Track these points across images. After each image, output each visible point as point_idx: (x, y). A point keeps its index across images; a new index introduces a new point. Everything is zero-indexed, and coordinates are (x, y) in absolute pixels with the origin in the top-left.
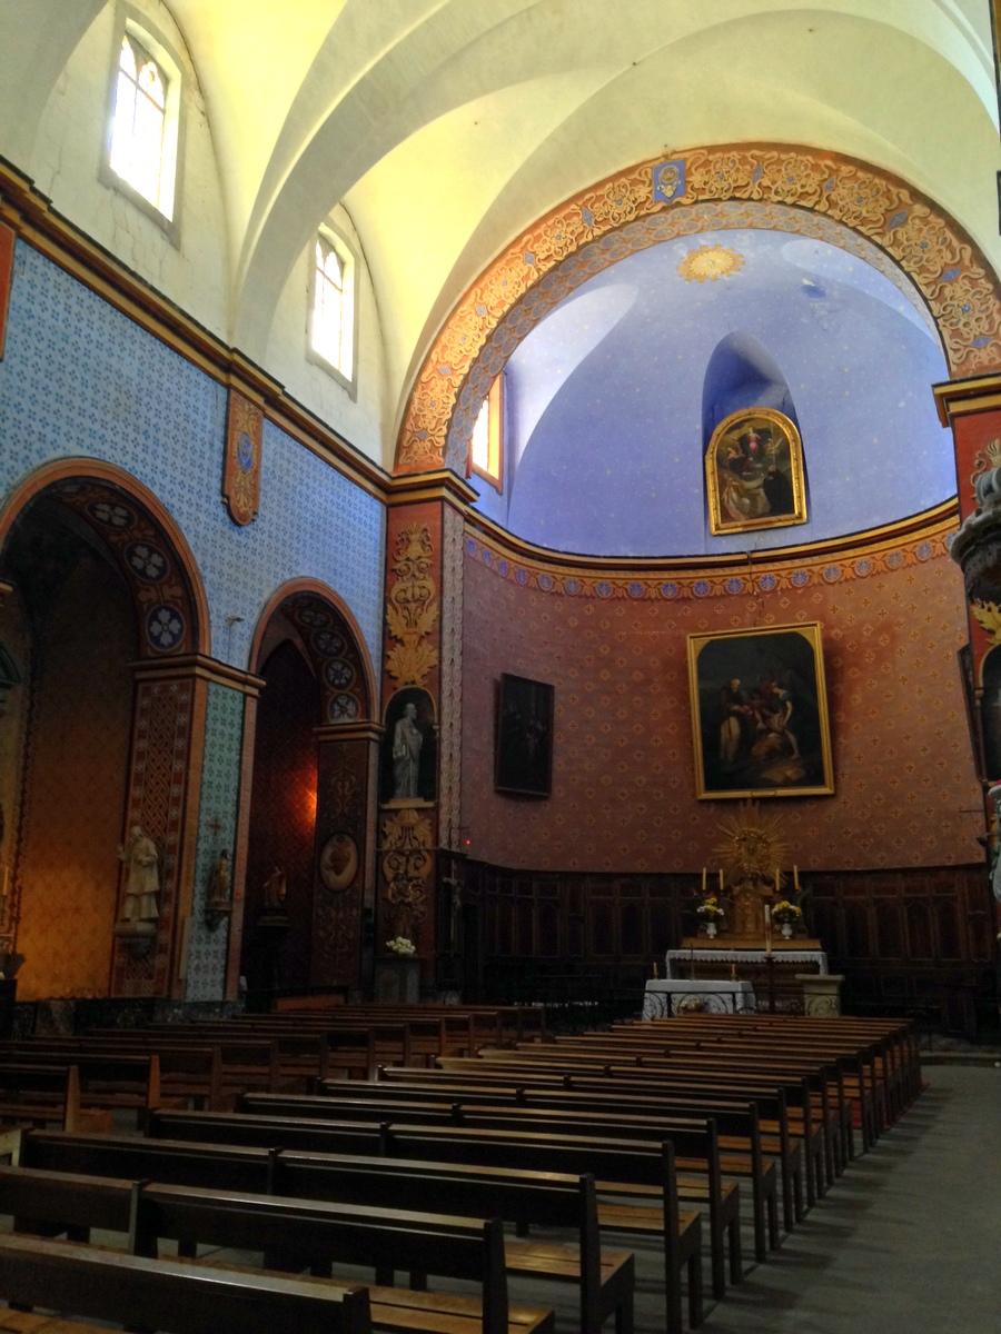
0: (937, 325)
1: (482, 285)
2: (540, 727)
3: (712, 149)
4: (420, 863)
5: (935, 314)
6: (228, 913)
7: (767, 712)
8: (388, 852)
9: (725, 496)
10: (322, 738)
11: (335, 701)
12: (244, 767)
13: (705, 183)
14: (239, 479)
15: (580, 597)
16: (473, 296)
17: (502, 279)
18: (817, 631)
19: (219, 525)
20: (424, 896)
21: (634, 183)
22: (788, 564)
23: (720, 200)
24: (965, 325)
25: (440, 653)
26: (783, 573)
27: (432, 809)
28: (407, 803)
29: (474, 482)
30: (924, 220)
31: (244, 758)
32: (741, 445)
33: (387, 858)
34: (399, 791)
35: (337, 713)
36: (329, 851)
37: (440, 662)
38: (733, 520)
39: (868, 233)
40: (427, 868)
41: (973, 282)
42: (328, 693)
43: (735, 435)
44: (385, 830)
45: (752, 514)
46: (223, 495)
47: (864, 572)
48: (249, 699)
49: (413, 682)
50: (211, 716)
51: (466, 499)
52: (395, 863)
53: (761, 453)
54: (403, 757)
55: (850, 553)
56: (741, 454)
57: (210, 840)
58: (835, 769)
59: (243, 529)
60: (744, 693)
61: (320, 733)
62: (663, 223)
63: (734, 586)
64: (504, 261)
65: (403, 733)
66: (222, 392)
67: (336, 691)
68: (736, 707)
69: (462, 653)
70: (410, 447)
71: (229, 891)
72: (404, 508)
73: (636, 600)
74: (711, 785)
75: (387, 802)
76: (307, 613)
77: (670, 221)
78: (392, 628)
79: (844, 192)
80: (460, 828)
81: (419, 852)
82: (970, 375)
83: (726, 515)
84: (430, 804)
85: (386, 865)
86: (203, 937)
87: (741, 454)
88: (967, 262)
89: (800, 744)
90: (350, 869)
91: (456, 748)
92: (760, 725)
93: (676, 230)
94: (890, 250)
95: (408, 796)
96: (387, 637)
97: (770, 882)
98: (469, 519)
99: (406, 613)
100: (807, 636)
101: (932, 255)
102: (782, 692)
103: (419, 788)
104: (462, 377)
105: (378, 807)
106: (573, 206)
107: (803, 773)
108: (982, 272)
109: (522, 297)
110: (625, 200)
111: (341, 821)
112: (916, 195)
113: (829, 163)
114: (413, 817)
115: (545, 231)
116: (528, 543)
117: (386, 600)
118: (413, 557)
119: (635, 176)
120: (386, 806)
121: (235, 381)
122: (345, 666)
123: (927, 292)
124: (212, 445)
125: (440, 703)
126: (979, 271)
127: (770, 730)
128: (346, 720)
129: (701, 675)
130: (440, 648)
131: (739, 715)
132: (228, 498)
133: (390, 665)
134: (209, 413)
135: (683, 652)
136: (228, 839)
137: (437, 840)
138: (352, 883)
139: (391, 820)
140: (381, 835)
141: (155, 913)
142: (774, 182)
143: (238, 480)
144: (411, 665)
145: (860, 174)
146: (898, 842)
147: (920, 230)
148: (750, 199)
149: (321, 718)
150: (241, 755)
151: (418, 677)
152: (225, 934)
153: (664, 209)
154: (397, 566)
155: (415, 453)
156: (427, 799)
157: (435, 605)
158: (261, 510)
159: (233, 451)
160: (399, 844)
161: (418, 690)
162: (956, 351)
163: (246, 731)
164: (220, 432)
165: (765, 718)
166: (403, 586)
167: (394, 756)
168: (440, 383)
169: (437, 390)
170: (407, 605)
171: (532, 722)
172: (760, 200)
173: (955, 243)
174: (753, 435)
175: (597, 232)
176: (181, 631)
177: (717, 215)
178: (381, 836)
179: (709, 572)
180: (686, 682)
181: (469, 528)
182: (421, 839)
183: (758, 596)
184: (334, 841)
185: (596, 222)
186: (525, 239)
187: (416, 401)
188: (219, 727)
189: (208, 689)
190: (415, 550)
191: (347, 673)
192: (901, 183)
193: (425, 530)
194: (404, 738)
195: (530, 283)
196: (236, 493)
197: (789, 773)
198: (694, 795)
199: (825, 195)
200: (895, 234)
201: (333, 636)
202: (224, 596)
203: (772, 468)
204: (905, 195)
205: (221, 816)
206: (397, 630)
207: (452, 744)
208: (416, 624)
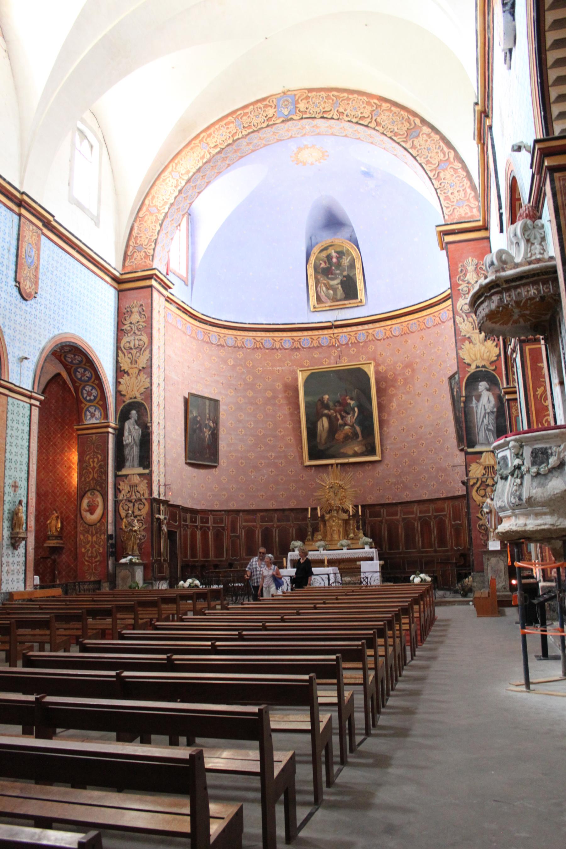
0: (437, 193)
1: (176, 161)
2: (212, 424)
3: (310, 90)
5: (436, 187)
6: (24, 539)
8: (122, 501)
9: (319, 289)
10: (80, 432)
11: (87, 410)
12: (31, 450)
13: (307, 108)
14: (25, 272)
15: (235, 347)
16: (170, 169)
18: (372, 366)
19: (13, 300)
20: (144, 526)
21: (266, 106)
22: (355, 328)
23: (315, 118)
24: (452, 194)
25: (151, 379)
26: (352, 334)
27: (148, 474)
28: (132, 470)
29: (171, 277)
30: (428, 135)
31: (31, 445)
32: (328, 260)
33: (121, 504)
34: (128, 464)
35: (89, 417)
36: (85, 502)
37: (151, 385)
38: (323, 302)
39: (398, 141)
40: (145, 510)
41: (455, 170)
42: (83, 405)
43: (324, 254)
44: (119, 487)
45: (335, 299)
46: (16, 281)
47: (397, 333)
48: (33, 407)
49: (135, 398)
50: (9, 419)
51: (166, 287)
54: (130, 443)
55: (389, 322)
56: (328, 265)
57: (12, 494)
58: (382, 445)
59: (28, 302)
60: (331, 404)
61: (78, 430)
63: (325, 341)
64: (189, 148)
65: (129, 428)
66: (16, 218)
67: (88, 404)
68: (326, 411)
69: (164, 380)
70: (132, 256)
71: (24, 526)
72: (128, 292)
73: (267, 349)
74: (312, 456)
76: (69, 356)
77: (286, 128)
78: (121, 365)
79: (384, 118)
80: (165, 485)
81: (141, 500)
82: (455, 221)
83: (319, 300)
84: (147, 471)
85: (121, 508)
86: (10, 553)
87: (328, 265)
88: (452, 160)
90: (99, 511)
91: (162, 437)
92: (340, 422)
93: (290, 134)
94: (410, 150)
95: (133, 466)
96: (119, 370)
97: (346, 511)
98: (168, 300)
99: (130, 356)
100: (366, 370)
101: (433, 155)
102: (352, 403)
104: (163, 214)
106: (230, 118)
107: (364, 449)
108: (460, 165)
109: (200, 168)
110: (260, 116)
111: (93, 482)
112: (424, 122)
113: (376, 101)
114: (136, 479)
115: (214, 132)
116: (203, 314)
117: (118, 348)
118: (134, 322)
119: (267, 102)
120: (120, 473)
121: (23, 212)
122: (93, 388)
123: (431, 175)
124: (9, 251)
125: (151, 410)
126: (458, 165)
127: (346, 424)
128: (94, 421)
129: (306, 393)
130: (151, 377)
131: (329, 417)
132: (19, 283)
133: (121, 388)
134: (7, 231)
135: (296, 379)
136: (23, 494)
137: (151, 493)
139: (123, 481)
140: (117, 490)
142: (345, 110)
143: (25, 272)
144: (133, 388)
145: (393, 108)
146: (416, 485)
147: (426, 141)
148: (332, 118)
149: (79, 420)
150: (29, 442)
151: (138, 395)
152: (24, 551)
153: (283, 121)
154: (124, 328)
155: (135, 259)
156: (145, 467)
157: (148, 351)
158: (40, 291)
159: (22, 254)
160: (128, 495)
161: (138, 403)
162: (447, 208)
163: (32, 427)
164: (14, 243)
165: (343, 417)
167: (124, 443)
168: (150, 218)
169: (149, 222)
170: (131, 351)
171: (207, 422)
172: (338, 119)
173: (445, 149)
174: (334, 254)
175: (245, 133)
177: (313, 127)
178: (117, 491)
179: (310, 333)
180: (297, 397)
181: (168, 305)
182: (142, 493)
183: (338, 347)
184: (89, 494)
185: (244, 127)
186: (202, 136)
187: (136, 228)
188: (15, 425)
189: (7, 402)
190: (135, 317)
191: (94, 392)
192: (415, 115)
193: (142, 305)
194: (130, 431)
195: (205, 160)
196: (24, 281)
197: (356, 449)
198: (302, 463)
199: (374, 119)
200: (413, 142)
201: (85, 370)
202: (17, 344)
203: (345, 273)
204: (418, 121)
205: (18, 480)
206: (125, 366)
207: (159, 435)
208: (136, 362)
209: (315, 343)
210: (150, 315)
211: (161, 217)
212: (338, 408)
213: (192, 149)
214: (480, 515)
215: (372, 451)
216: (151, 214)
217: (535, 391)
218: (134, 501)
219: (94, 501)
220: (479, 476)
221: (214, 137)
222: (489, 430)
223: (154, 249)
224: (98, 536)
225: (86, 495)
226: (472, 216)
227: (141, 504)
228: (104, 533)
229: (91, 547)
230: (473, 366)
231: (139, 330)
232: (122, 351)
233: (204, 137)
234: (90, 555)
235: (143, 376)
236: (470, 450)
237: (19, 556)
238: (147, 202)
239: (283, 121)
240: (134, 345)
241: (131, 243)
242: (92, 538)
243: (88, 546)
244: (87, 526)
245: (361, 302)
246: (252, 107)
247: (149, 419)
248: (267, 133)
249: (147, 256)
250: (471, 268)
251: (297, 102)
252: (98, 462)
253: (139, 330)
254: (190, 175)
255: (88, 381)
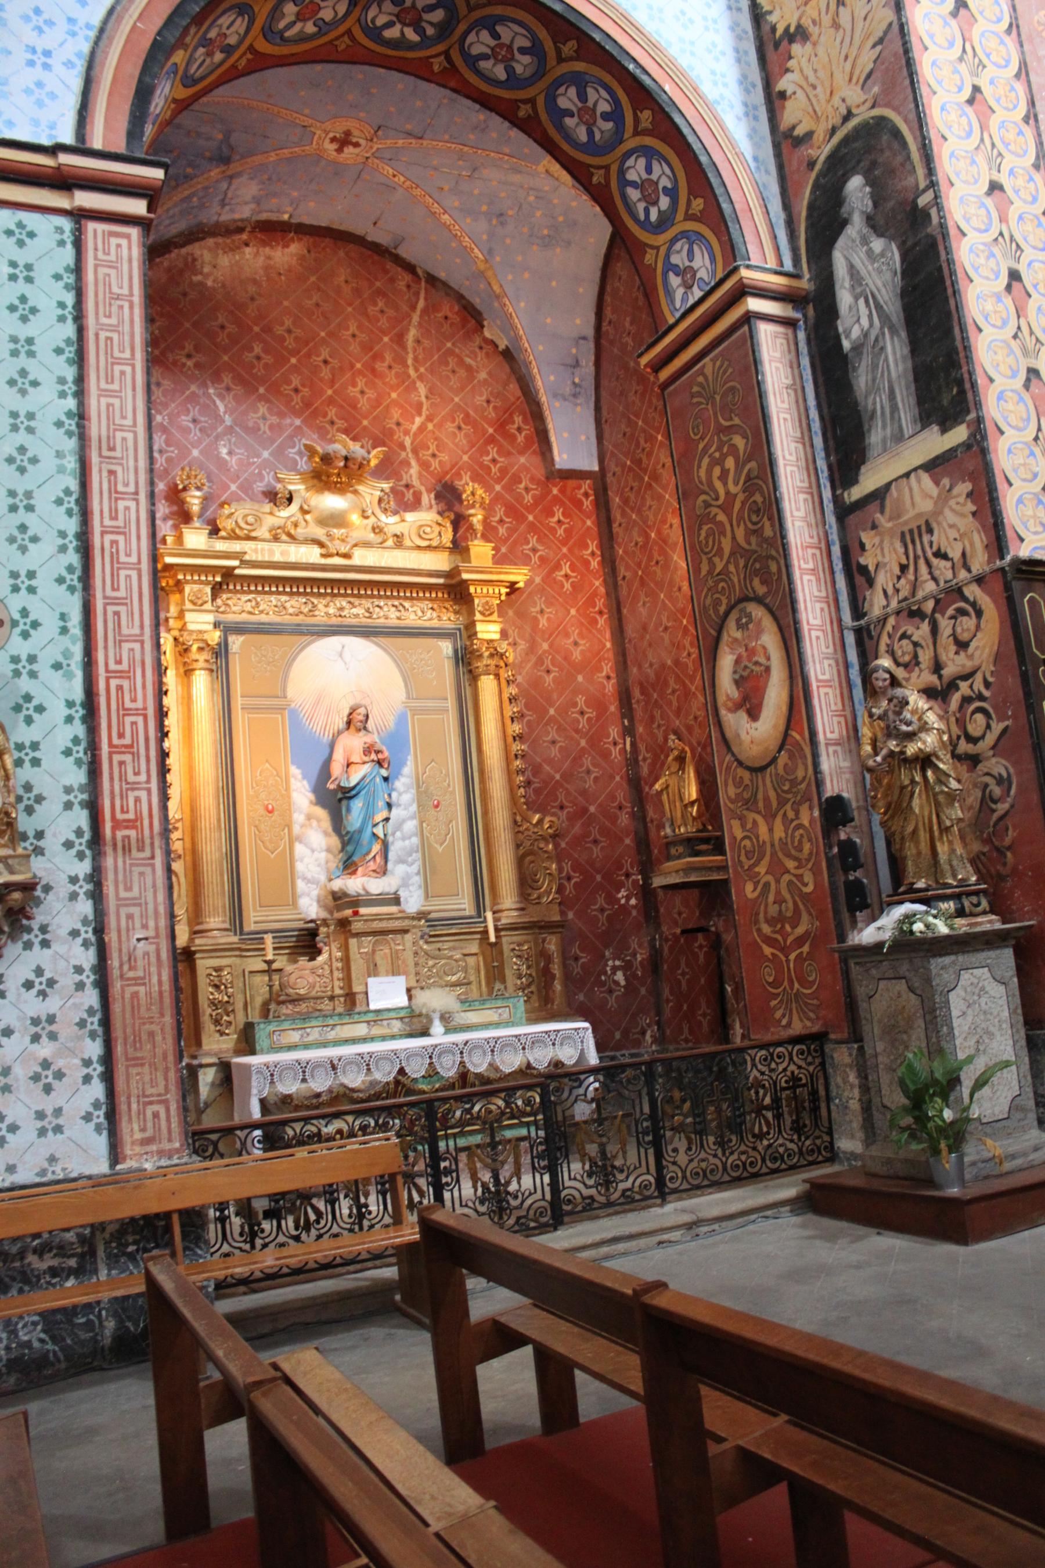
4: (968, 623)
20: (997, 727)
27: (967, 446)
28: (901, 456)
34: (875, 437)
36: (726, 662)
40: (987, 638)
42: (649, 257)
44: (862, 561)
49: (848, 116)
65: (851, 267)
84: (959, 434)
90: (775, 695)
95: (899, 438)
103: (920, 401)
105: (837, 500)
114: (921, 496)
120: (856, 493)
137: (998, 537)
138: (786, 735)
139: (874, 527)
167: (846, 345)
178: (860, 580)
182: (955, 554)
184: (732, 632)
218: (930, 605)
219: (751, 652)
224: (791, 814)
225: (725, 637)
227: (962, 612)
228: (807, 798)
229: (772, 868)
234: (773, 910)
237: (41, 984)
242: (771, 830)
243: (762, 869)
244: (747, 775)
247: (921, 171)
252: (739, 467)
255: (618, 137)
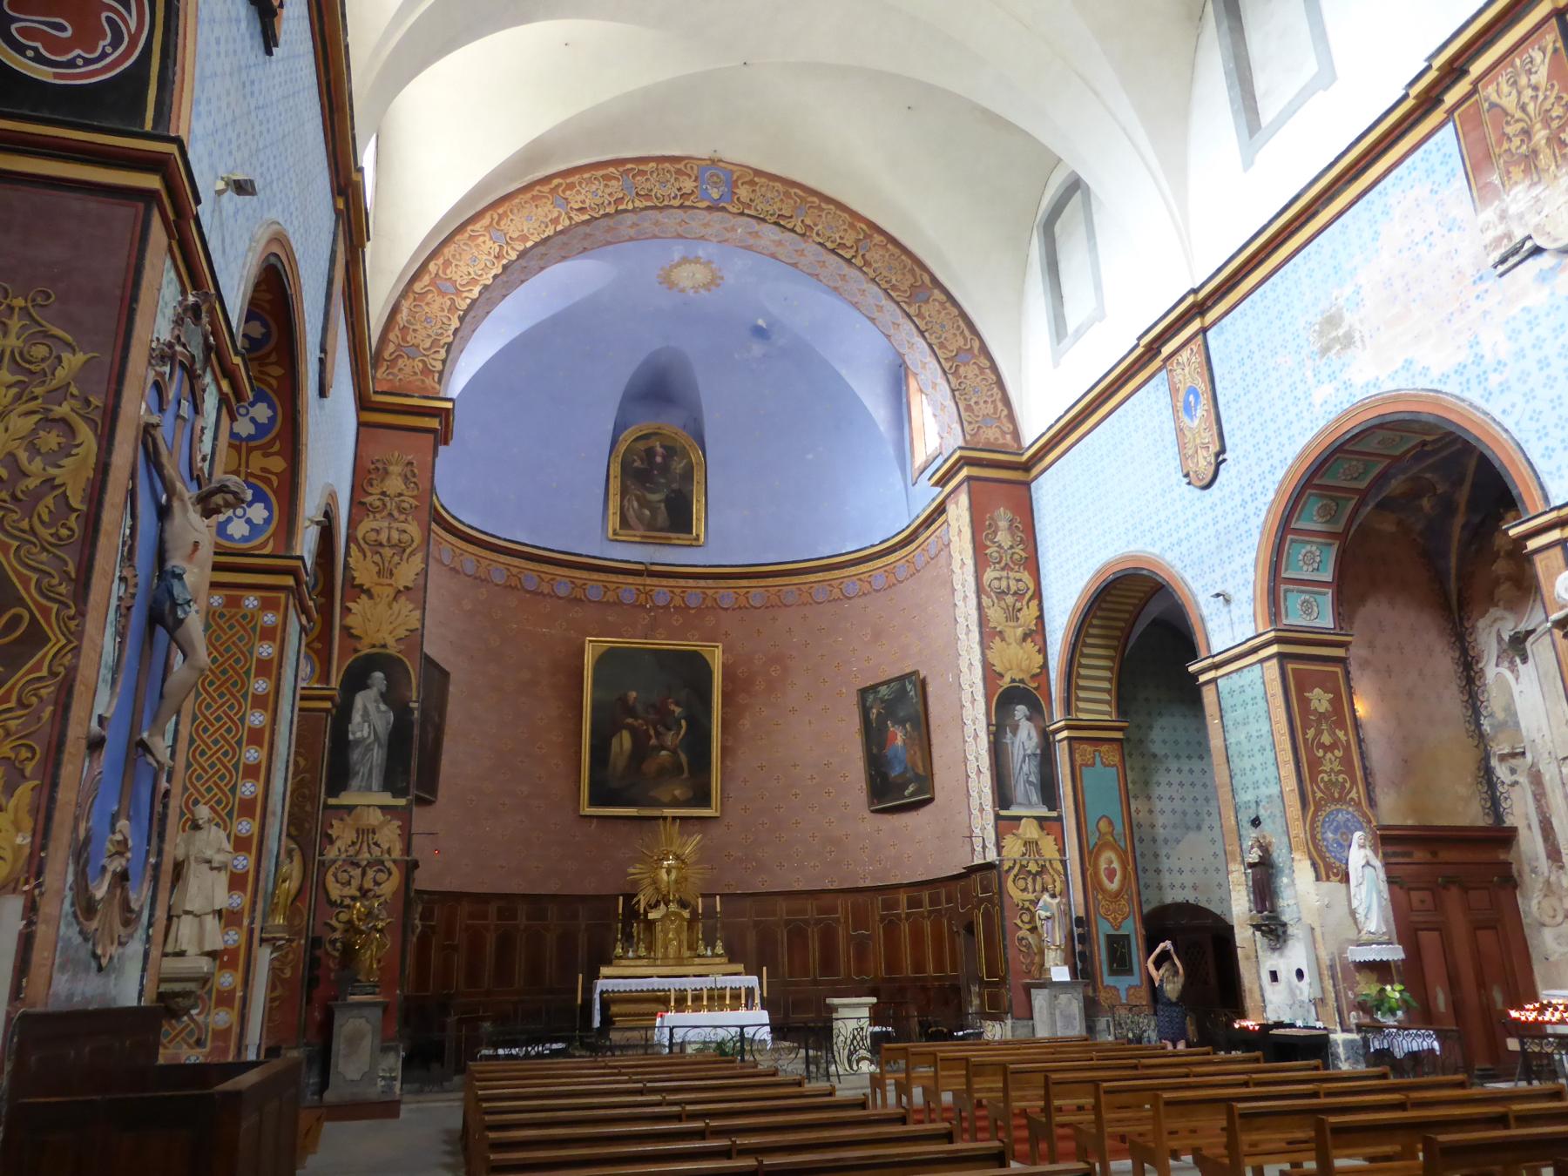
1: (500, 211)
3: (758, 173)
4: (382, 877)
7: (661, 729)
8: (334, 862)
16: (486, 221)
17: (525, 212)
18: (718, 653)
23: (764, 220)
26: (677, 591)
30: (942, 304)
33: (332, 870)
34: (355, 783)
41: (981, 369)
45: (651, 526)
49: (384, 646)
52: (344, 877)
53: (665, 469)
54: (364, 739)
55: (744, 583)
60: (639, 708)
62: (699, 221)
64: (529, 195)
68: (630, 720)
70: (393, 362)
75: (336, 795)
78: (356, 574)
79: (877, 257)
81: (382, 863)
83: (624, 523)
85: (330, 878)
89: (689, 764)
92: (653, 741)
95: (369, 789)
99: (377, 558)
101: (949, 336)
102: (678, 710)
106: (612, 169)
107: (690, 794)
109: (549, 238)
112: (936, 282)
114: (376, 817)
118: (390, 492)
119: (681, 166)
123: (947, 366)
126: (985, 363)
127: (663, 748)
131: (634, 732)
133: (350, 621)
141: (219, 946)
146: (781, 865)
148: (792, 230)
151: (391, 641)
153: (709, 208)
154: (368, 500)
157: (419, 557)
160: (352, 851)
161: (390, 657)
165: (658, 734)
166: (375, 525)
167: (351, 737)
168: (439, 300)
169: (436, 306)
172: (803, 235)
173: (967, 332)
174: (659, 450)
175: (637, 204)
176: (267, 521)
179: (603, 577)
182: (385, 847)
183: (651, 609)
186: (556, 182)
190: (394, 484)
193: (410, 463)
195: (559, 228)
197: (677, 792)
203: (675, 486)
208: (392, 574)
209: (611, 597)
210: (428, 486)
211: (464, 305)
212: (652, 717)
213: (534, 198)
214: (1018, 922)
215: (703, 799)
216: (442, 293)
217: (1305, 734)
220: (1017, 856)
221: (579, 192)
222: (1031, 783)
223: (444, 362)
226: (1004, 445)
230: (1007, 679)
231: (401, 510)
232: (359, 546)
233: (559, 185)
235: (404, 606)
236: (1003, 813)
238: (432, 267)
239: (709, 208)
240: (389, 539)
241: (392, 336)
245: (697, 538)
246: (653, 164)
248: (671, 219)
249: (427, 371)
250: (1003, 524)
251: (735, 184)
253: (401, 510)
254: (529, 244)
